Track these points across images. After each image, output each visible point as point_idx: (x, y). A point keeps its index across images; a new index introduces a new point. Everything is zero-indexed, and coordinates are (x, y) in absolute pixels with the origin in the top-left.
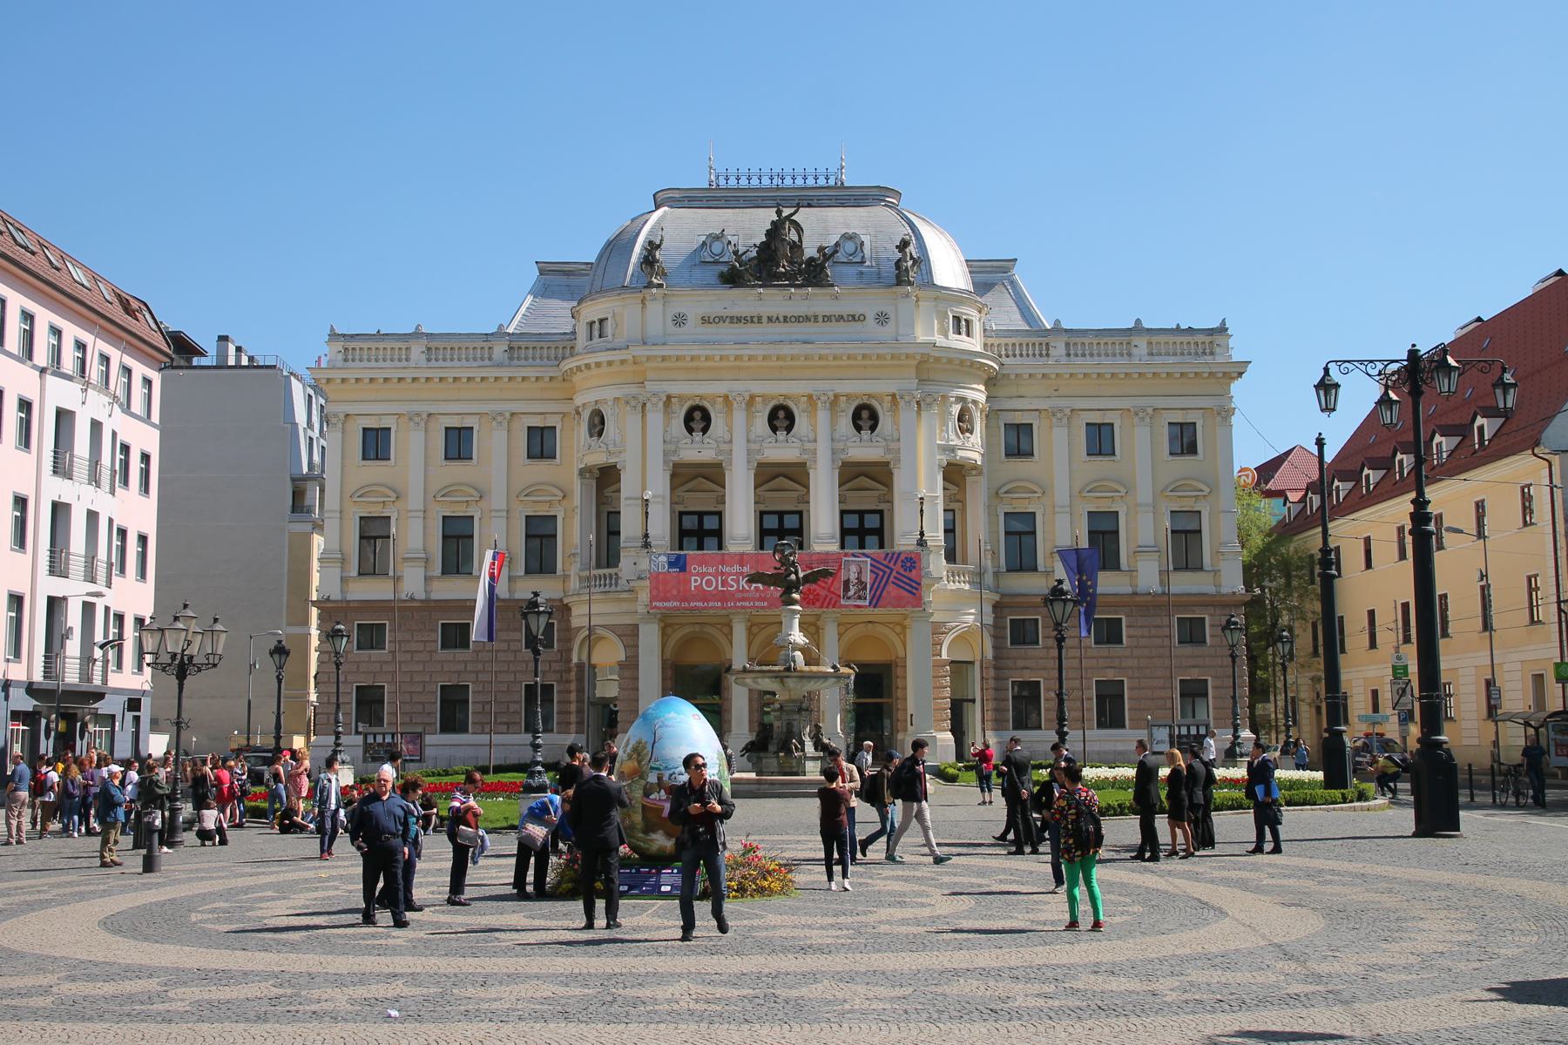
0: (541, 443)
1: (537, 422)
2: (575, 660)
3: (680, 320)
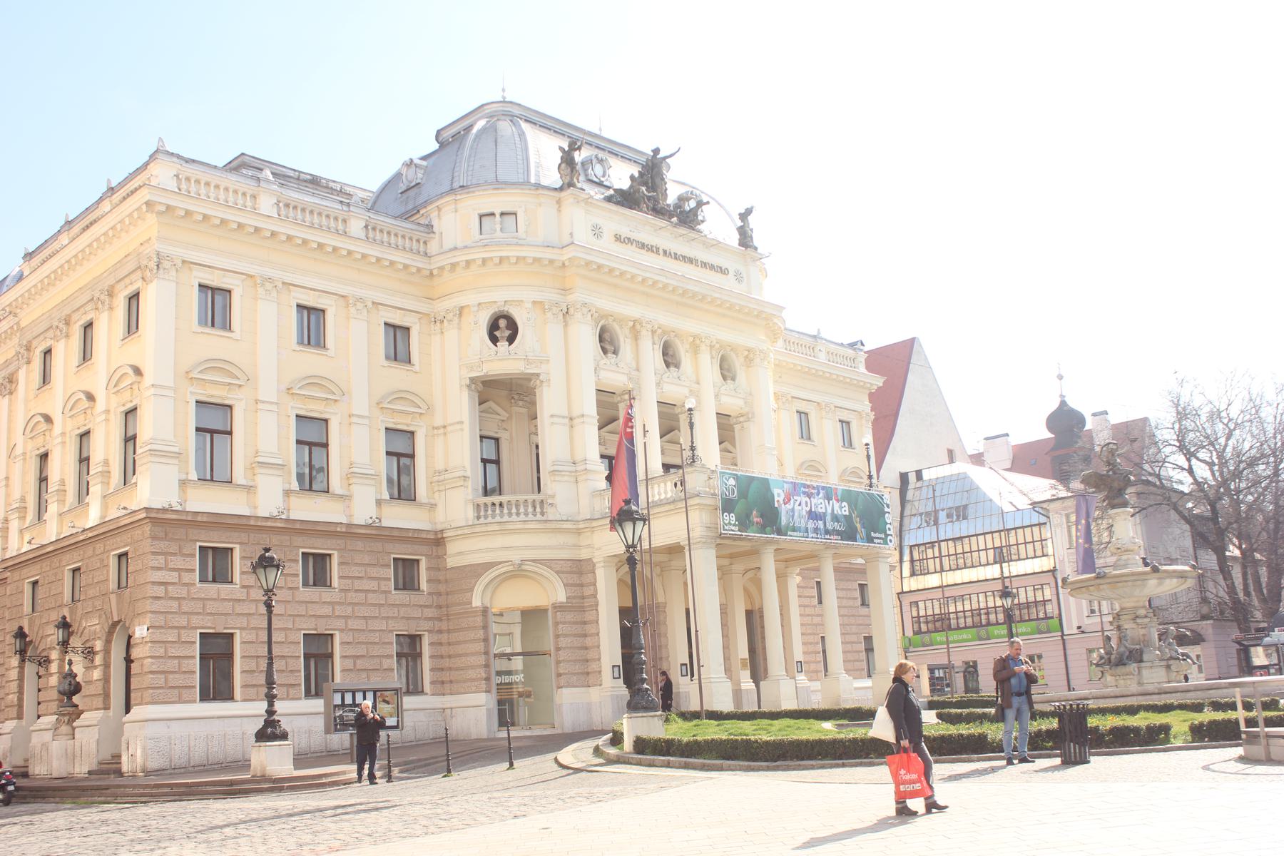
0: (398, 341)
1: (397, 319)
2: (476, 602)
3: (597, 231)
